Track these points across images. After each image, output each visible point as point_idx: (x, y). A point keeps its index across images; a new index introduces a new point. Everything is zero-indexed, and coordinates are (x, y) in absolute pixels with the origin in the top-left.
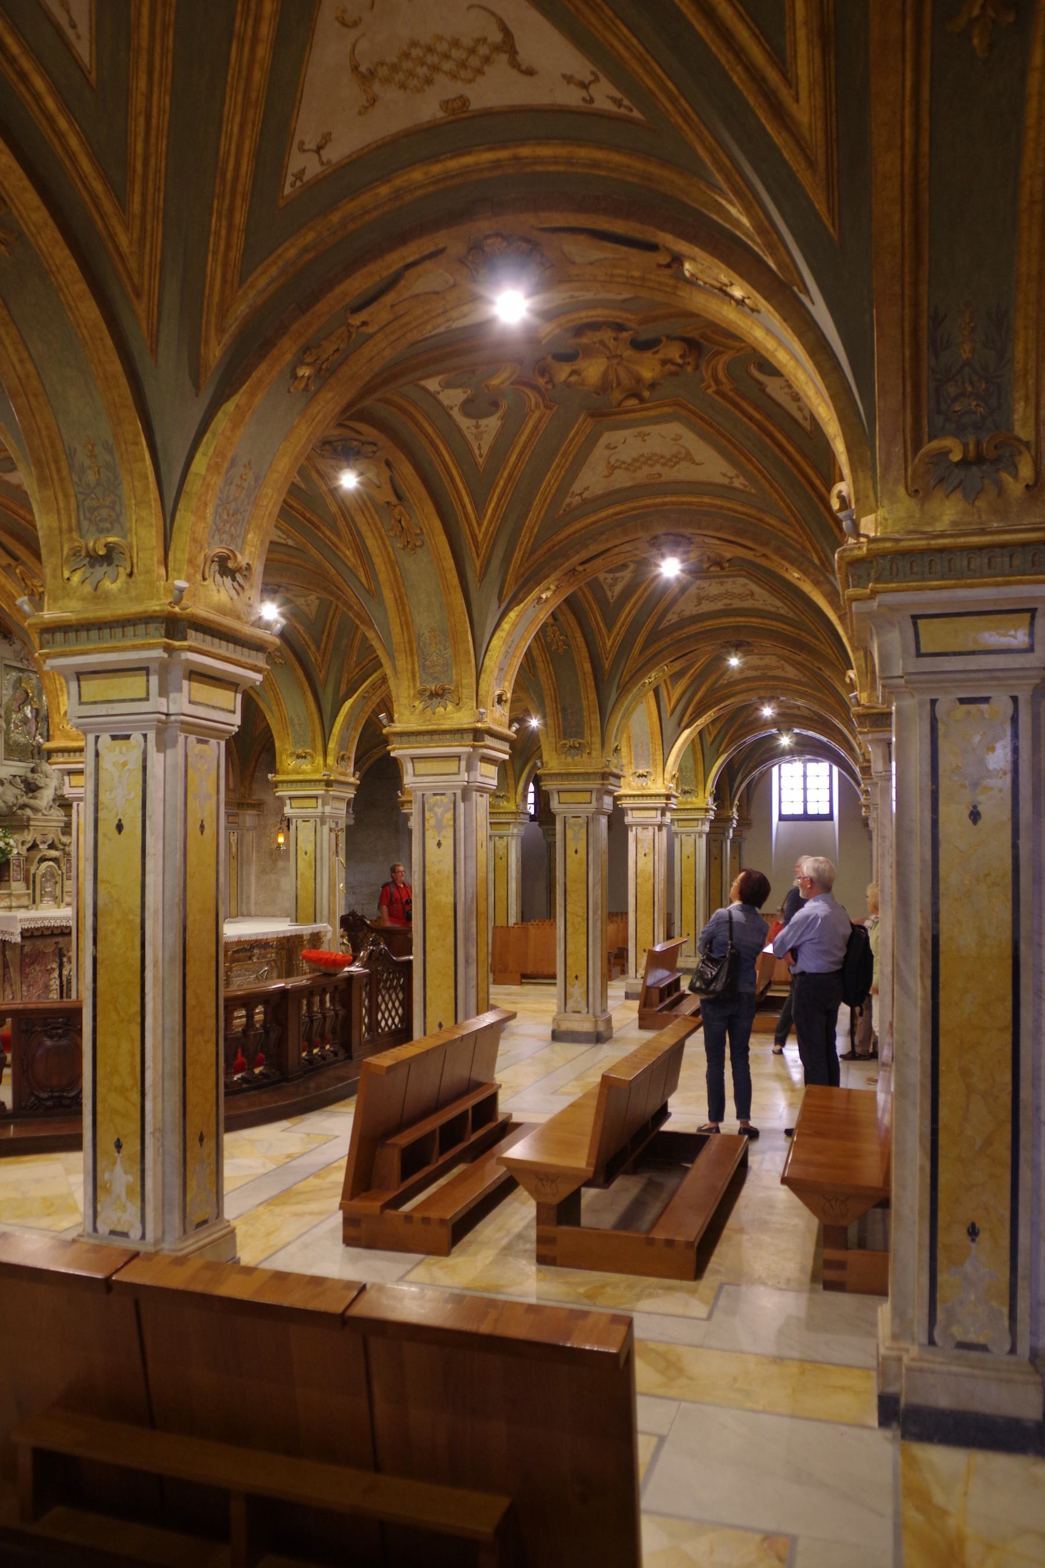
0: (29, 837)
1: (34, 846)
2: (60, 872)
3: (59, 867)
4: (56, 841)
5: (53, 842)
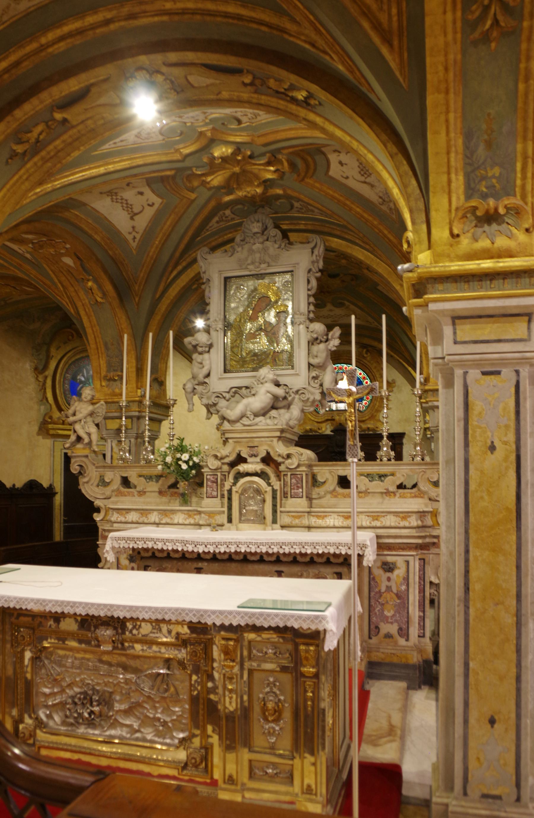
2: (269, 489)
3: (269, 484)
4: (272, 454)
5: (268, 453)
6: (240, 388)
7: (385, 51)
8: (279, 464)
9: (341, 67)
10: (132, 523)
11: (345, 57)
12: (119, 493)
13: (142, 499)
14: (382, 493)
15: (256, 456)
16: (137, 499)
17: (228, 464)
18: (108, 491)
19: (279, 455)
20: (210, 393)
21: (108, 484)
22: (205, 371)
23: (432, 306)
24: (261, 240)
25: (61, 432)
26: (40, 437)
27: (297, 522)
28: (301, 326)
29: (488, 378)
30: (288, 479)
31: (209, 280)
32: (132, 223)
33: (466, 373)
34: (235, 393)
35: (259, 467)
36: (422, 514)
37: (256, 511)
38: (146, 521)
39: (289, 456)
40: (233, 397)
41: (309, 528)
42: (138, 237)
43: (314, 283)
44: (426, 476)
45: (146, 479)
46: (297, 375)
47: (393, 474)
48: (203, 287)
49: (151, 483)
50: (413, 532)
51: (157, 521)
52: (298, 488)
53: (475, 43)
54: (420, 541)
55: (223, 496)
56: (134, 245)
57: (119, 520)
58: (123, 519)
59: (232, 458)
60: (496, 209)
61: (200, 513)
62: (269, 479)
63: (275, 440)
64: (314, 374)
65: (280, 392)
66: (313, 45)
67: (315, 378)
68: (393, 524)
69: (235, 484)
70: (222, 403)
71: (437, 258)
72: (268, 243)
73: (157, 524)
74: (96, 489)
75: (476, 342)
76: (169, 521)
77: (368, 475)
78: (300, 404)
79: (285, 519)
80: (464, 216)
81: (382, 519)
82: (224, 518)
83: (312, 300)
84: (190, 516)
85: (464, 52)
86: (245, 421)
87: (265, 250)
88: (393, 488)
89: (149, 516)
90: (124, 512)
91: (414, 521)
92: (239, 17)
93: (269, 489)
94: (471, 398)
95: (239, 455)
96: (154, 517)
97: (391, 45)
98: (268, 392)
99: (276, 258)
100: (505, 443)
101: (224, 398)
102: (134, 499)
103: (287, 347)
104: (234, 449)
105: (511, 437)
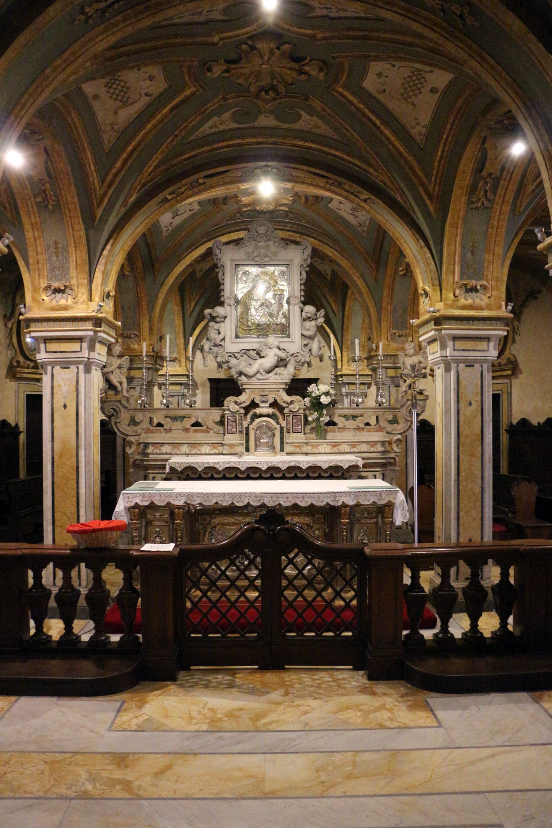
0: (245, 398)
1: (254, 405)
2: (278, 426)
3: (278, 423)
4: (279, 401)
5: (275, 401)
6: (249, 350)
7: (428, 202)
8: (284, 408)
9: (399, 199)
10: (166, 454)
11: (403, 194)
12: (148, 431)
13: (169, 435)
14: (354, 429)
15: (266, 402)
16: (164, 435)
17: (244, 408)
18: (138, 429)
19: (284, 402)
20: (224, 353)
21: (138, 424)
22: (221, 336)
23: (443, 332)
24: (265, 239)
25: (25, 375)
26: (8, 380)
27: (297, 450)
28: (296, 307)
29: (468, 368)
30: (290, 419)
31: (223, 266)
32: (172, 220)
33: (458, 365)
34: (244, 353)
35: (271, 411)
36: (383, 443)
37: (268, 443)
38: (178, 452)
39: (292, 402)
40: (242, 356)
41: (307, 454)
42: (171, 229)
43: (304, 275)
44: (384, 417)
45: (171, 419)
46: (293, 342)
47: (362, 416)
48: (217, 270)
49: (176, 423)
50: (379, 455)
51: (188, 452)
52: (298, 426)
53: (472, 209)
54: (384, 461)
55: (241, 432)
56: (165, 234)
57: (155, 452)
58: (158, 452)
59: (248, 403)
60: (476, 286)
61: (223, 445)
62: (278, 420)
63: (281, 390)
64: (305, 342)
65: (282, 354)
66: (385, 184)
67: (305, 345)
68: (366, 450)
69: (251, 423)
70: (233, 361)
71: (447, 306)
72: (271, 243)
73: (188, 455)
74: (127, 428)
75: (464, 350)
76: (198, 452)
77: (345, 416)
78: (294, 363)
79: (288, 448)
80: (461, 287)
81: (358, 447)
82: (242, 449)
83: (303, 287)
84: (214, 448)
85: (466, 212)
86: (259, 376)
87: (267, 247)
88: (362, 425)
89: (180, 448)
90: (158, 445)
91: (380, 448)
92: (343, 159)
93: (278, 426)
94: (460, 379)
95: (253, 401)
96: (185, 449)
97: (432, 202)
98: (276, 355)
99: (275, 254)
100: (476, 401)
101: (236, 357)
102: (161, 435)
103: (284, 321)
104: (249, 397)
105: (479, 399)
